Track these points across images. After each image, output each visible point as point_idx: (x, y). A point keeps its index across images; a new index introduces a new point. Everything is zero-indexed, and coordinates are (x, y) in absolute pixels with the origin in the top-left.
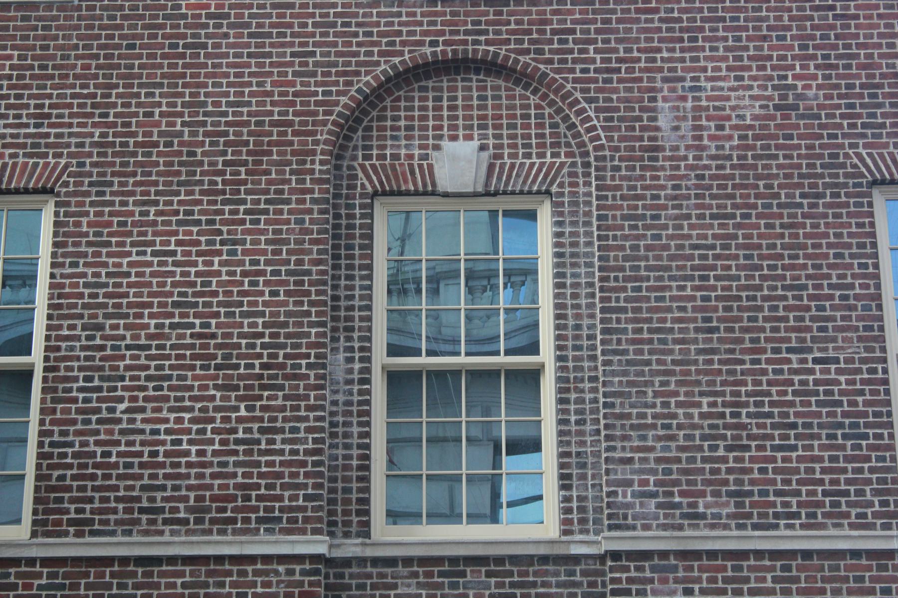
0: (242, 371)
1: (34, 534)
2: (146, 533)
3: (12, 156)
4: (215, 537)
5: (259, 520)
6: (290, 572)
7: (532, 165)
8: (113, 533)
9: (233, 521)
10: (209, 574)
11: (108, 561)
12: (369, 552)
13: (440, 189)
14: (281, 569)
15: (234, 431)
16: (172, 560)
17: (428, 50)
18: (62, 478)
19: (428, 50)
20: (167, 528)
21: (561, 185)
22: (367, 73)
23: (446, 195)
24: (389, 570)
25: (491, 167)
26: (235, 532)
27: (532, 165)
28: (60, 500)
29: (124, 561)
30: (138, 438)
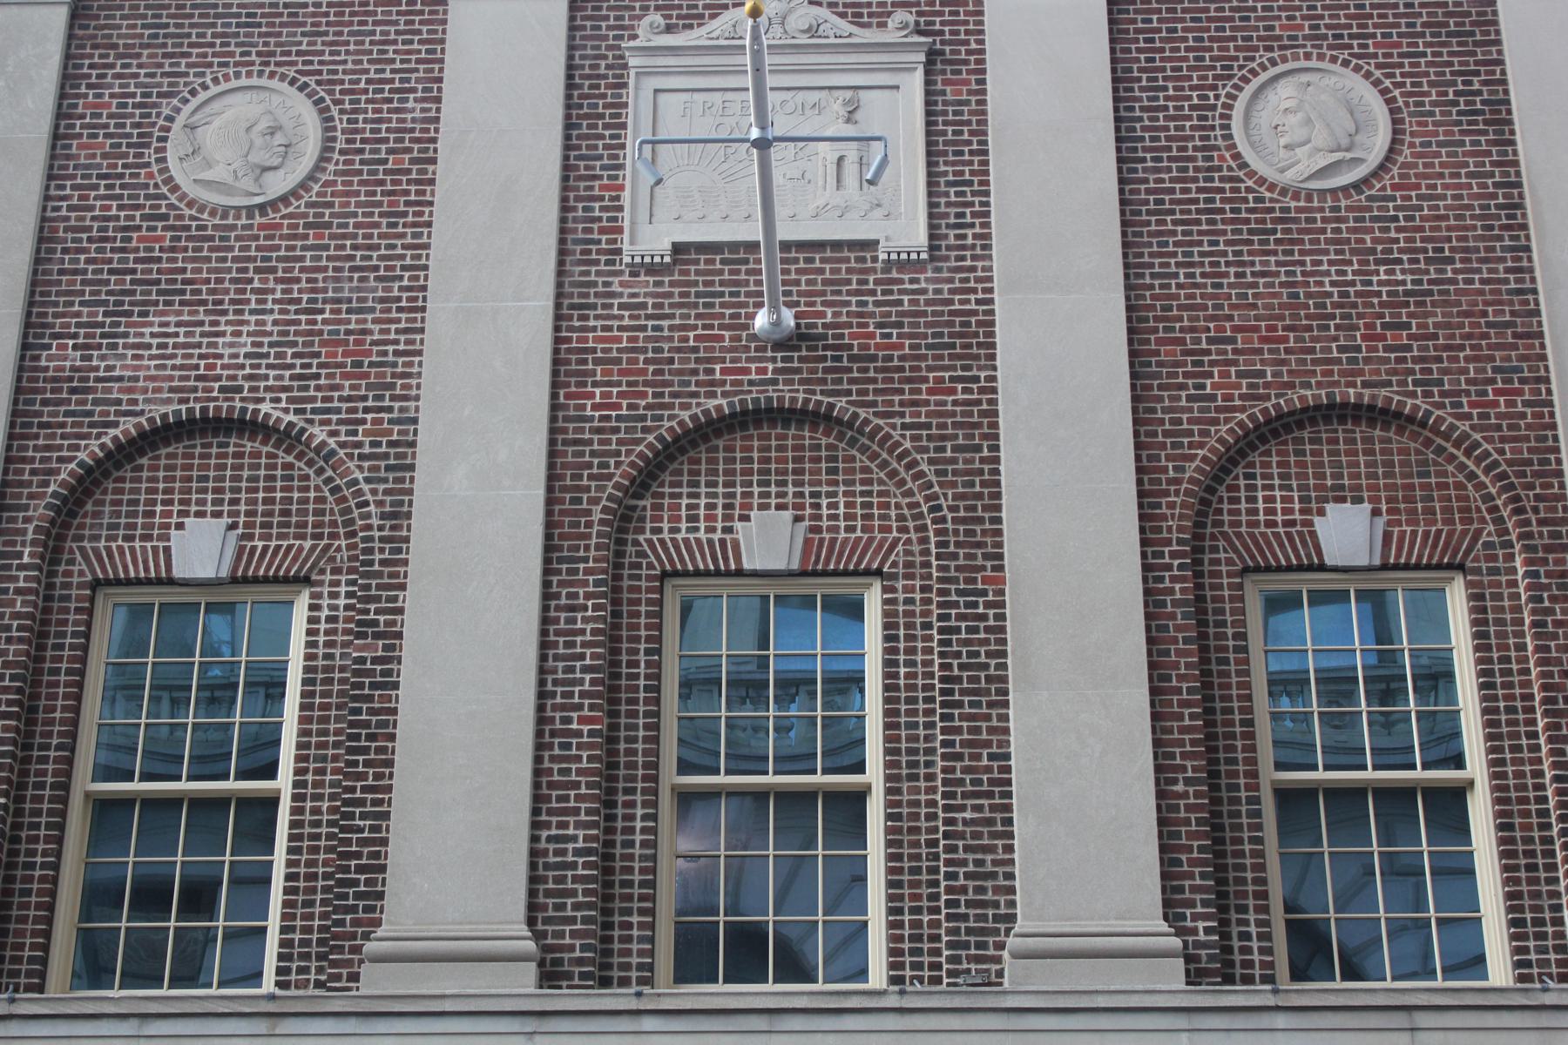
7: (1439, 532)
13: (1328, 561)
21: (1476, 559)
23: (1335, 569)
27: (1439, 532)
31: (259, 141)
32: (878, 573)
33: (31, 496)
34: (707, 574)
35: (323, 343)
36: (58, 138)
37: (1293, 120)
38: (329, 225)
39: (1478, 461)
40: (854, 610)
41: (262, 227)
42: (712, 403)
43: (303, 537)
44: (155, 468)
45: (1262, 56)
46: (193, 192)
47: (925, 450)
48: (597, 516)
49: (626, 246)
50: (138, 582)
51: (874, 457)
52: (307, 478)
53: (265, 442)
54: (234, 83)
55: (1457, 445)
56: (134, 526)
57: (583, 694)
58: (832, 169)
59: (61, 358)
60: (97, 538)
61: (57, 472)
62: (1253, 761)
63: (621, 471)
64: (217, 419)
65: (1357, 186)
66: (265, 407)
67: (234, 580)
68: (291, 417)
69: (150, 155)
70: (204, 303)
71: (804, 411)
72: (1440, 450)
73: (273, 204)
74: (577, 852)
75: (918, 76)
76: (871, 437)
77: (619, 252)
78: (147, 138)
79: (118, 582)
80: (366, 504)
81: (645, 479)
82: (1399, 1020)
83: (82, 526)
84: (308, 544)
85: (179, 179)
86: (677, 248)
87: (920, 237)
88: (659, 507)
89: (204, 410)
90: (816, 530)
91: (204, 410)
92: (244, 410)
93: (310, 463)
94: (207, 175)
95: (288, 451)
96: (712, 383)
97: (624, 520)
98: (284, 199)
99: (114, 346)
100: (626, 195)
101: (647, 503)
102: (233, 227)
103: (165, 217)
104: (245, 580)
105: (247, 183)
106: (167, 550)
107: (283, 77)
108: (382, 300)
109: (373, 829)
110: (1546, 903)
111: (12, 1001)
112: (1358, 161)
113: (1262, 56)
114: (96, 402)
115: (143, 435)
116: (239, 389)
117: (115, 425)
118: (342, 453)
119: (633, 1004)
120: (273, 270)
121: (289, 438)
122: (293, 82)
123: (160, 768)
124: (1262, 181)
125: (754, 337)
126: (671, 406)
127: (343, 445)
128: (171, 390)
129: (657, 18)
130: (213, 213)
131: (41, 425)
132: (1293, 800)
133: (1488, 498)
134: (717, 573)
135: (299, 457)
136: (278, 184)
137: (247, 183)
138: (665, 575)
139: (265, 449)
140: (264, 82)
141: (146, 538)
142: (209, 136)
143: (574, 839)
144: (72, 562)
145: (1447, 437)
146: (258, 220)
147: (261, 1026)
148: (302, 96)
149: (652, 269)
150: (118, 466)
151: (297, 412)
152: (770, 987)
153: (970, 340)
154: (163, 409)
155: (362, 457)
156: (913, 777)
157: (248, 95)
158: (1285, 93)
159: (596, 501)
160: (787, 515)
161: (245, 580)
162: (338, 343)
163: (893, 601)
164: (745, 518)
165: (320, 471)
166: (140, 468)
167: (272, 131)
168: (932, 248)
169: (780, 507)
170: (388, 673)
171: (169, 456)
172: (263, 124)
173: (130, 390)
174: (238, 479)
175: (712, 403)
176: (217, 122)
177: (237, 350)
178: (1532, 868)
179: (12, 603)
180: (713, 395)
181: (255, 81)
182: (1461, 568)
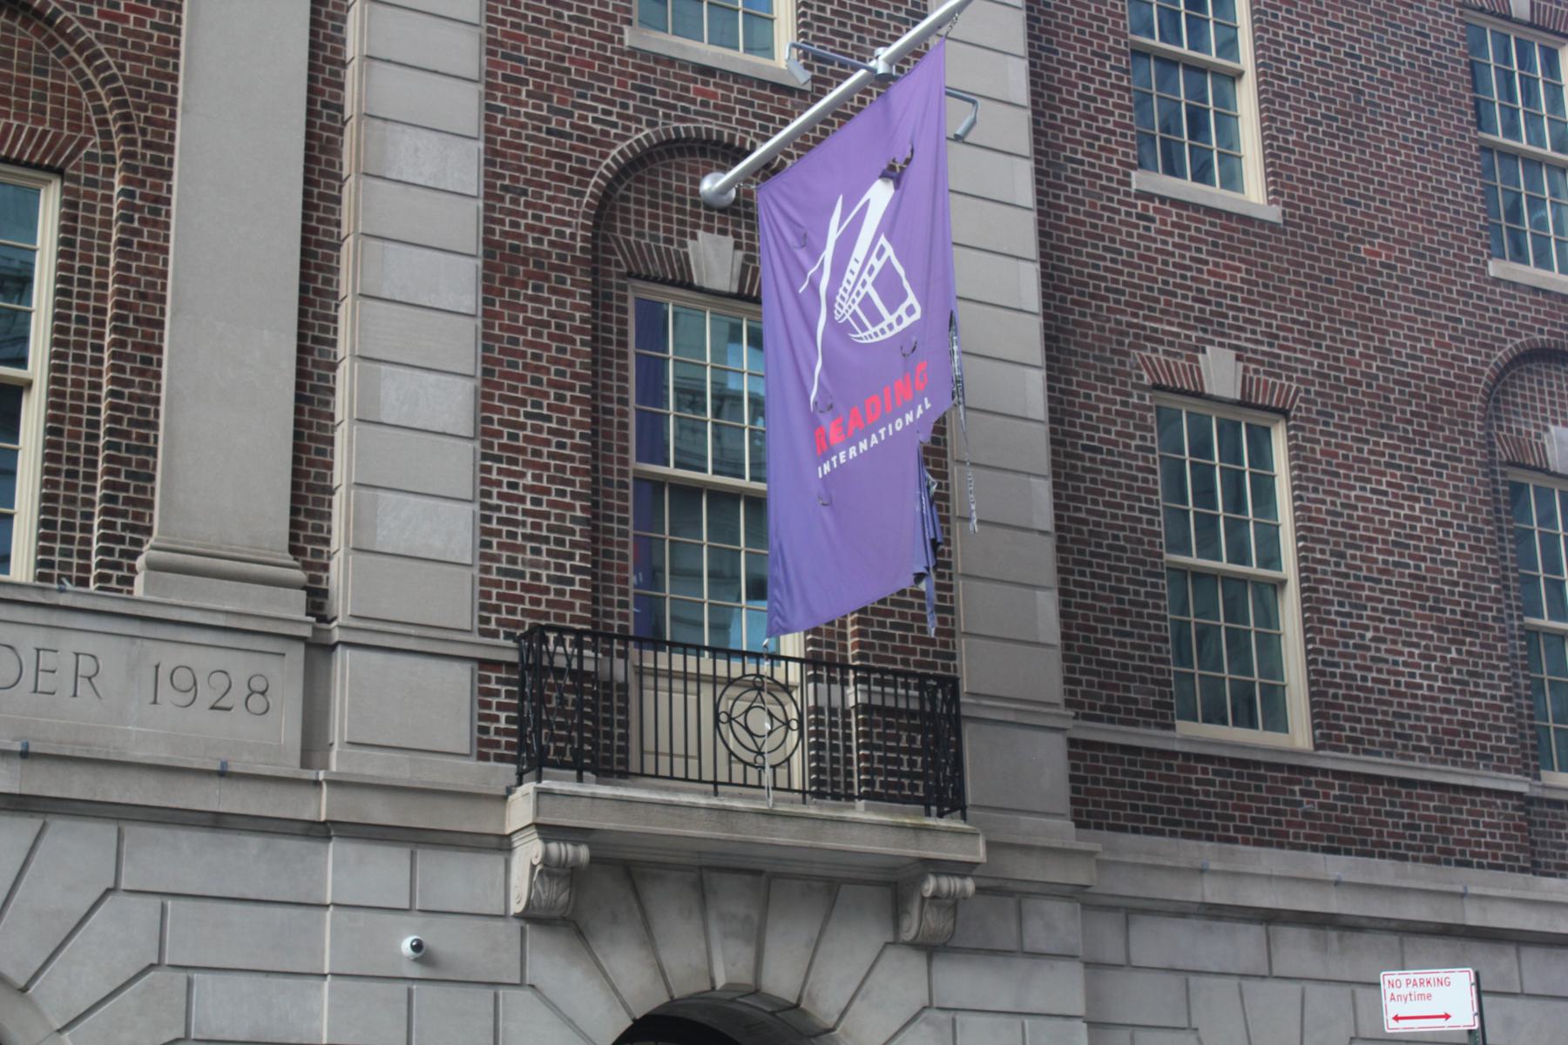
0: (1448, 615)
1: (1317, 747)
2: (1403, 757)
3: (1256, 371)
4: (1449, 767)
5: (1479, 756)
6: (1505, 806)
7: (45, 133)
8: (1378, 754)
9: (1459, 754)
10: (1453, 800)
11: (1377, 779)
12: (1538, 792)
14: (1499, 802)
15: (1449, 671)
16: (1424, 784)
17: (1538, 337)
18: (1335, 696)
19: (1538, 337)
20: (1417, 755)
21: (77, 167)
22: (1500, 348)
24: (1559, 812)
26: (1464, 765)
27: (45, 133)
28: (1336, 717)
29: (1391, 780)
30: (1385, 667)
39: (98, 71)
55: (80, 50)
72: (62, 52)
110: (79, 509)
133: (100, 110)
145: (71, 40)
178: (72, 474)
182: (60, 172)
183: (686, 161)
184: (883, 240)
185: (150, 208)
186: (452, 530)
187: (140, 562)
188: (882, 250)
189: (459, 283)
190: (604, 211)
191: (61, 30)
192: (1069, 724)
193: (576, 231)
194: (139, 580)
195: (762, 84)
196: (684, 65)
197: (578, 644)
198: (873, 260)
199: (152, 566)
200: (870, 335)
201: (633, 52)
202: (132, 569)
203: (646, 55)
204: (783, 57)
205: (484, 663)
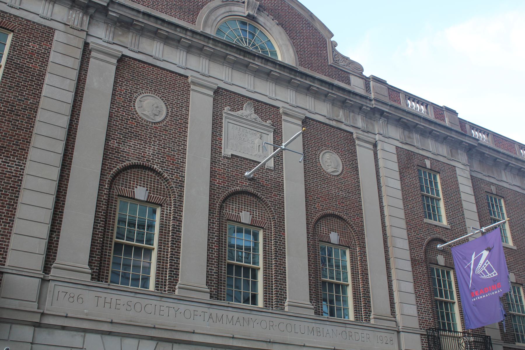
25: (149, 195)
31: (155, 109)
32: (263, 228)
33: (107, 173)
34: (234, 221)
35: (166, 156)
36: (113, 95)
37: (329, 161)
38: (167, 131)
40: (154, 212)
41: (154, 127)
42: (238, 188)
43: (161, 196)
44: (131, 173)
45: (324, 148)
46: (141, 115)
47: (272, 206)
48: (217, 205)
49: (223, 152)
50: (127, 197)
51: (263, 205)
52: (161, 183)
53: (153, 173)
54: (148, 94)
55: (350, 226)
56: (127, 185)
57: (215, 241)
58: (258, 147)
59: (114, 144)
60: (119, 185)
61: (113, 169)
62: (112, 236)
63: (222, 197)
64: (145, 166)
65: (338, 176)
66: (155, 166)
67: (147, 202)
68: (160, 170)
69: (132, 104)
70: (143, 140)
71: (253, 194)
72: (347, 226)
73: (157, 123)
74: (214, 273)
75: (272, 133)
76: (263, 202)
77: (221, 153)
78: (131, 101)
79: (123, 196)
80: (175, 192)
81: (224, 201)
82: (344, 325)
83: (116, 182)
84: (162, 197)
85: (138, 111)
86: (232, 155)
87: (273, 165)
88: (226, 206)
89: (143, 164)
90: (253, 217)
91: (143, 164)
92: (151, 166)
93: (162, 180)
94: (144, 113)
95: (158, 176)
96: (237, 184)
97: (221, 207)
98: (159, 122)
99: (125, 145)
100: (223, 141)
101: (225, 205)
102: (149, 126)
103: (135, 119)
104: (149, 202)
105: (152, 117)
106: (134, 192)
107: (159, 96)
108: (178, 150)
109: (177, 261)
111: (109, 285)
112: (338, 171)
113: (324, 148)
114: (121, 156)
115: (130, 165)
116: (150, 161)
117: (125, 162)
118: (170, 180)
119: (227, 305)
120: (157, 137)
121: (159, 174)
122: (160, 98)
123: (120, 237)
124: (324, 170)
125: (244, 177)
126: (230, 187)
127: (170, 178)
128: (136, 157)
129: (228, 107)
130: (145, 121)
131: (110, 158)
132: (118, 246)
133: (353, 236)
134: (236, 222)
135: (160, 178)
136: (158, 119)
137: (152, 117)
138: (227, 220)
139: (153, 175)
140: (155, 96)
141: (129, 188)
142: (145, 104)
143: (214, 270)
144: (114, 189)
145: (349, 224)
146: (154, 125)
147: (159, 299)
148: (162, 101)
149: (227, 158)
150: (124, 171)
151: (162, 169)
152: (250, 305)
153: (280, 187)
154: (135, 161)
155: (174, 182)
156: (269, 268)
157: (152, 98)
158: (327, 156)
159: (217, 202)
160: (249, 213)
161: (149, 202)
162: (169, 156)
163: (265, 234)
164: (241, 212)
165: (164, 183)
166: (128, 172)
167: (157, 107)
168: (274, 168)
169: (247, 211)
170: (179, 229)
171: (134, 171)
172: (155, 105)
173: (128, 155)
174: (148, 180)
175: (238, 188)
176: (146, 102)
177: (150, 152)
179: (103, 196)
180: (237, 186)
181: (153, 95)
183: (434, 242)
184: (487, 261)
185: (363, 253)
186: (413, 310)
187: (177, 287)
188: (487, 263)
189: (408, 265)
190: (426, 252)
191: (347, 223)
192: (503, 344)
193: (423, 256)
194: (177, 291)
195: (444, 228)
196: (433, 225)
197: (433, 331)
198: (485, 264)
199: (179, 288)
200: (485, 277)
201: (426, 223)
202: (175, 288)
203: (428, 223)
204: (444, 222)
205: (421, 334)
